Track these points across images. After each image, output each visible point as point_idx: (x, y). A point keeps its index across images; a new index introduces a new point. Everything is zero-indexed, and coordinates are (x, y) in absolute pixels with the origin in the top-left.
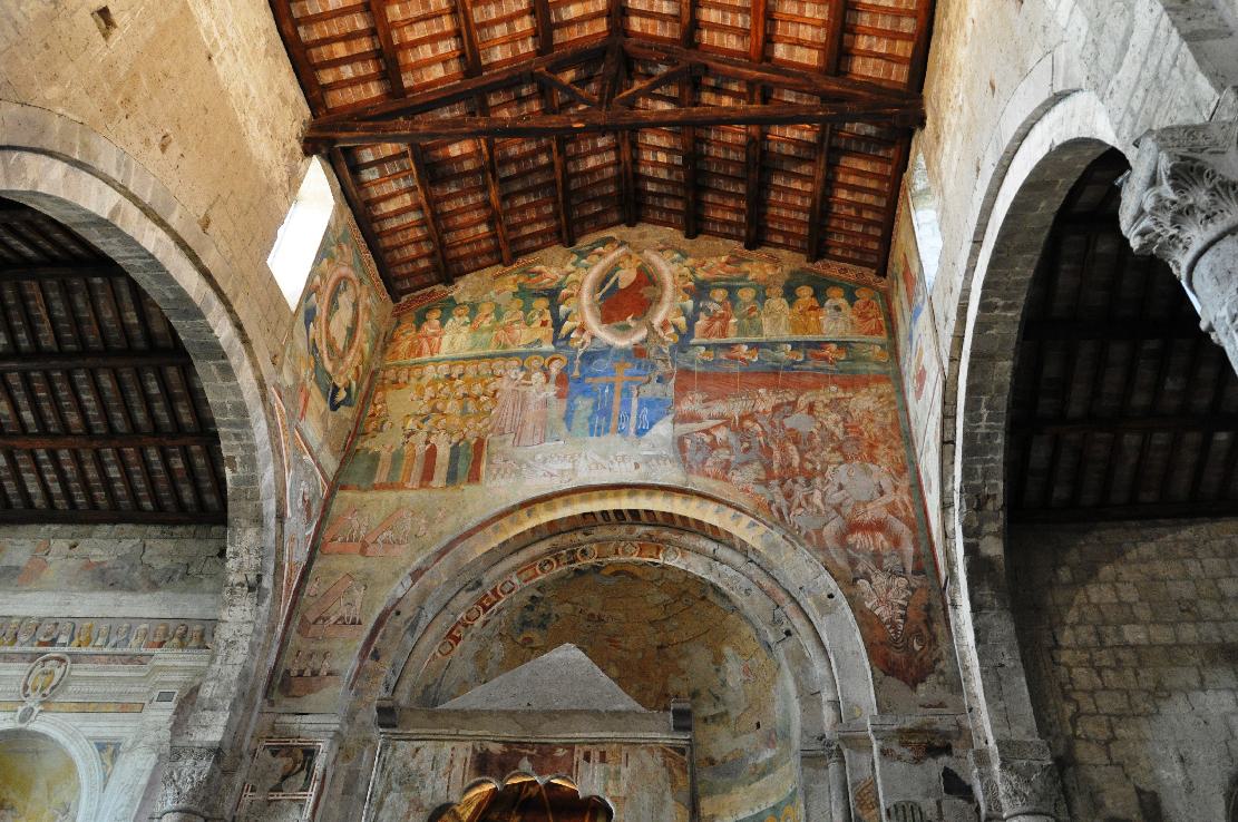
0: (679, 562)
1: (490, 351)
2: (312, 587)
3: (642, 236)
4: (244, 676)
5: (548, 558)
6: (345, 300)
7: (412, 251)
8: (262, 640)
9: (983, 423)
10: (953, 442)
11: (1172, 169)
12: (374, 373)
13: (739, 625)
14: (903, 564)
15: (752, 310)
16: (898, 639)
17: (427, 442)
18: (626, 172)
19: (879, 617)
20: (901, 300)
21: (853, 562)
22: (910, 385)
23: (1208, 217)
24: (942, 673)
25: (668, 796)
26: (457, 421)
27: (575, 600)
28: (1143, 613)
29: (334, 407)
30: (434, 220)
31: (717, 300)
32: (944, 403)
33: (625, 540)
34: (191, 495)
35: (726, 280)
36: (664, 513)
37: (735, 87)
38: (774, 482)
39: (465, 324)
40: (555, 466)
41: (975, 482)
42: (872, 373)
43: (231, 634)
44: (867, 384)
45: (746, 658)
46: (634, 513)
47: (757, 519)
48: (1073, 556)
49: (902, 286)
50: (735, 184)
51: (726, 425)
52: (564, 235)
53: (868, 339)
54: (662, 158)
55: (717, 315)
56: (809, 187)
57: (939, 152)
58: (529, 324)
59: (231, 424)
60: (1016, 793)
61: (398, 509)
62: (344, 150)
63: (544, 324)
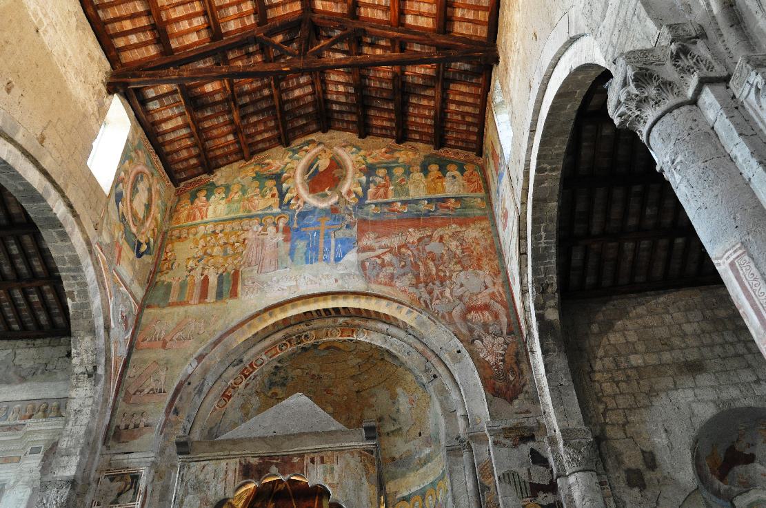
1: (241, 214)
2: (131, 372)
3: (332, 138)
4: (88, 432)
5: (284, 342)
6: (142, 186)
7: (185, 153)
8: (99, 408)
9: (543, 241)
10: (526, 254)
11: (634, 75)
12: (165, 233)
14: (501, 329)
15: (403, 180)
17: (202, 275)
18: (319, 97)
19: (488, 362)
20: (491, 171)
21: (471, 330)
22: (499, 221)
23: (656, 103)
24: (527, 392)
25: (364, 480)
26: (221, 260)
27: (302, 367)
28: (641, 347)
29: (139, 255)
30: (198, 133)
33: (332, 326)
34: (45, 319)
35: (386, 163)
37: (383, 43)
39: (223, 198)
40: (285, 284)
41: (541, 277)
42: (477, 215)
43: (78, 406)
44: (473, 222)
46: (337, 310)
47: (412, 308)
48: (600, 317)
49: (491, 162)
50: (388, 103)
51: (390, 252)
52: (283, 140)
53: (473, 194)
54: (341, 89)
56: (432, 103)
57: (508, 78)
58: (263, 196)
59: (69, 270)
60: (573, 460)
61: (185, 317)
62: (137, 91)
63: (273, 196)
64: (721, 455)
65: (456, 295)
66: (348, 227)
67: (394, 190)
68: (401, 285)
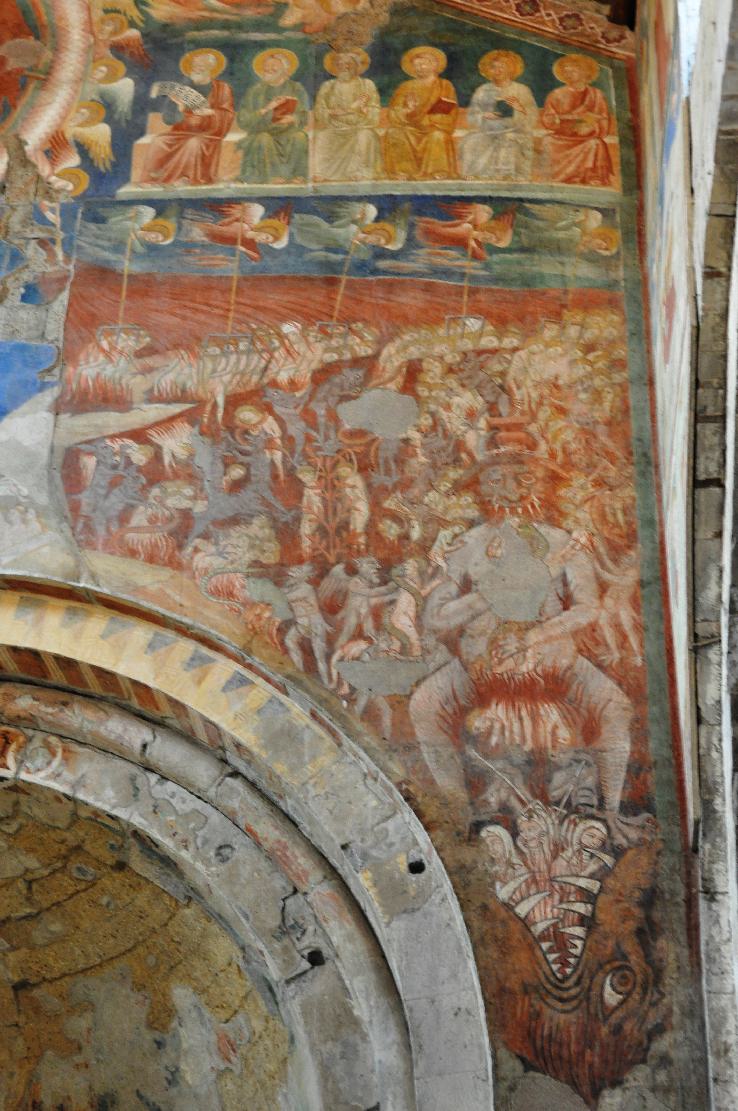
0: (57, 776)
13: (204, 935)
15: (287, 108)
16: (566, 978)
19: (526, 923)
21: (475, 782)
24: (665, 1061)
31: (196, 78)
32: (696, 384)
35: (226, 25)
36: (15, 650)
38: (300, 572)
42: (572, 287)
44: (557, 316)
45: (224, 1015)
47: (249, 667)
51: (190, 417)
55: (194, 121)
65: (439, 624)
66: (31, 294)
67: (248, 150)
68: (217, 562)
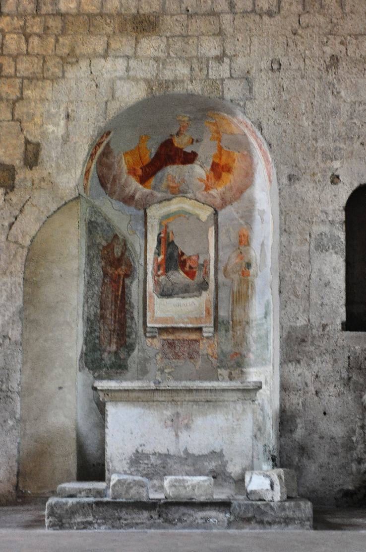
64: (151, 149)
